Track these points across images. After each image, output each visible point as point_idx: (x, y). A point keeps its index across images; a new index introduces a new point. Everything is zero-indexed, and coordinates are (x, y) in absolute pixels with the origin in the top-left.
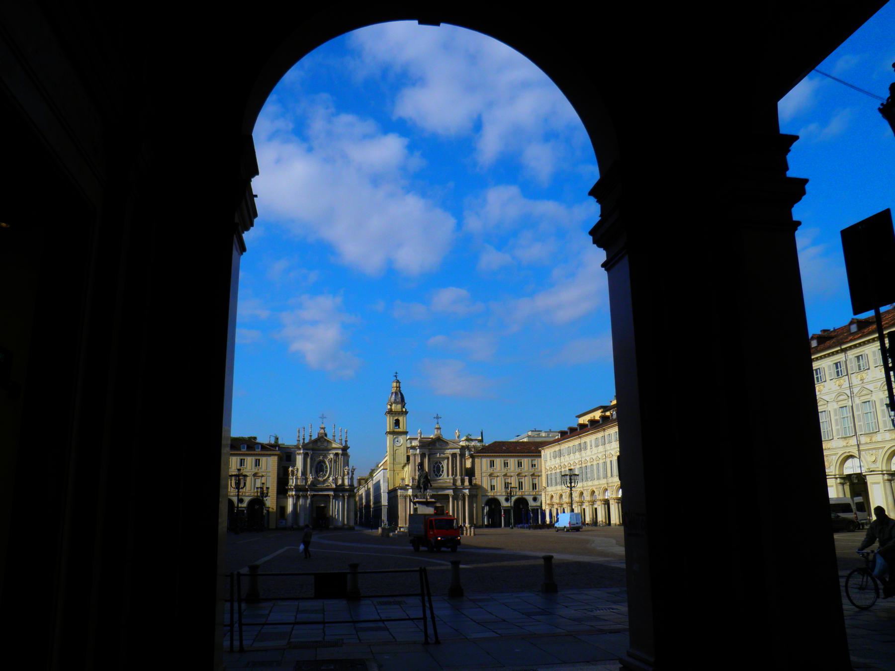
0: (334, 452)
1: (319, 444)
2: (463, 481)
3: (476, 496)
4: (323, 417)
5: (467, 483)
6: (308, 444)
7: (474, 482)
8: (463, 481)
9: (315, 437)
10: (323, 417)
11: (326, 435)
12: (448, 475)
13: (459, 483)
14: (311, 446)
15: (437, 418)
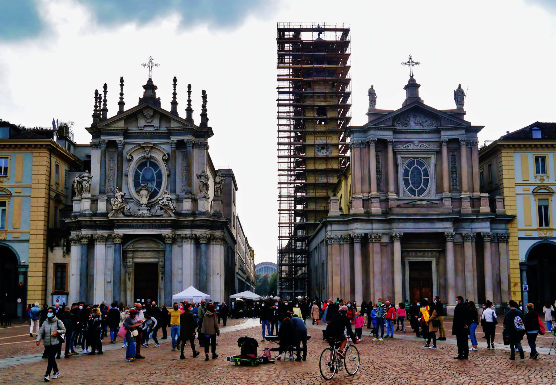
0: (174, 139)
1: (142, 123)
2: (475, 202)
3: (505, 239)
4: (150, 64)
5: (485, 209)
6: (115, 120)
7: (499, 205)
8: (475, 202)
9: (131, 103)
10: (150, 64)
11: (157, 102)
12: (439, 189)
13: (466, 207)
14: (121, 124)
15: (411, 63)
